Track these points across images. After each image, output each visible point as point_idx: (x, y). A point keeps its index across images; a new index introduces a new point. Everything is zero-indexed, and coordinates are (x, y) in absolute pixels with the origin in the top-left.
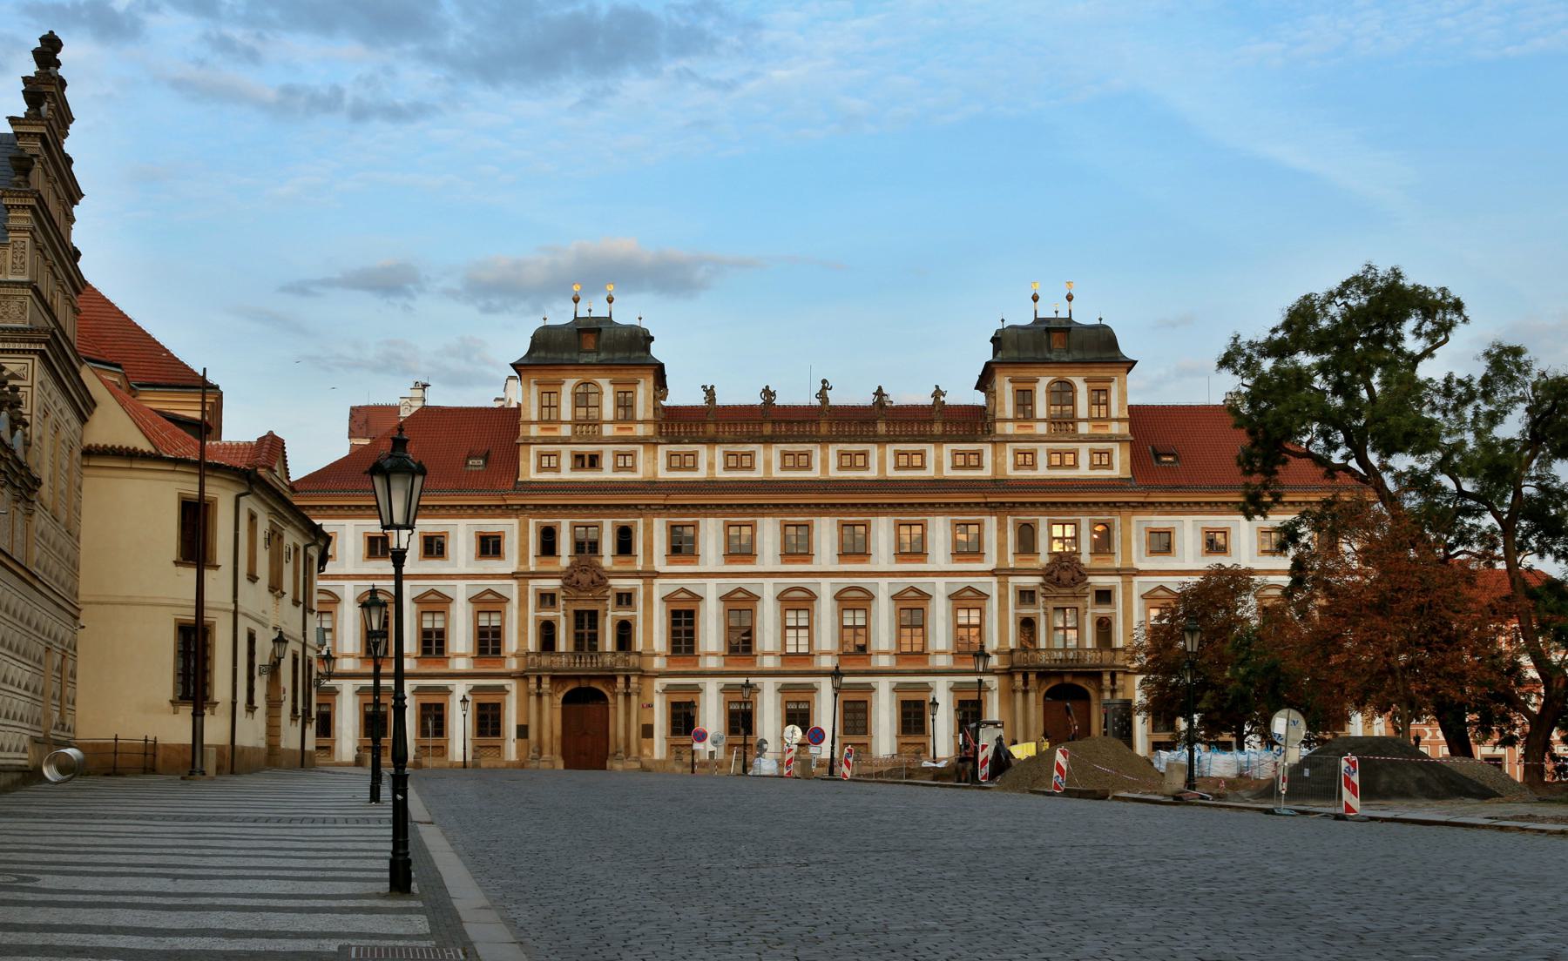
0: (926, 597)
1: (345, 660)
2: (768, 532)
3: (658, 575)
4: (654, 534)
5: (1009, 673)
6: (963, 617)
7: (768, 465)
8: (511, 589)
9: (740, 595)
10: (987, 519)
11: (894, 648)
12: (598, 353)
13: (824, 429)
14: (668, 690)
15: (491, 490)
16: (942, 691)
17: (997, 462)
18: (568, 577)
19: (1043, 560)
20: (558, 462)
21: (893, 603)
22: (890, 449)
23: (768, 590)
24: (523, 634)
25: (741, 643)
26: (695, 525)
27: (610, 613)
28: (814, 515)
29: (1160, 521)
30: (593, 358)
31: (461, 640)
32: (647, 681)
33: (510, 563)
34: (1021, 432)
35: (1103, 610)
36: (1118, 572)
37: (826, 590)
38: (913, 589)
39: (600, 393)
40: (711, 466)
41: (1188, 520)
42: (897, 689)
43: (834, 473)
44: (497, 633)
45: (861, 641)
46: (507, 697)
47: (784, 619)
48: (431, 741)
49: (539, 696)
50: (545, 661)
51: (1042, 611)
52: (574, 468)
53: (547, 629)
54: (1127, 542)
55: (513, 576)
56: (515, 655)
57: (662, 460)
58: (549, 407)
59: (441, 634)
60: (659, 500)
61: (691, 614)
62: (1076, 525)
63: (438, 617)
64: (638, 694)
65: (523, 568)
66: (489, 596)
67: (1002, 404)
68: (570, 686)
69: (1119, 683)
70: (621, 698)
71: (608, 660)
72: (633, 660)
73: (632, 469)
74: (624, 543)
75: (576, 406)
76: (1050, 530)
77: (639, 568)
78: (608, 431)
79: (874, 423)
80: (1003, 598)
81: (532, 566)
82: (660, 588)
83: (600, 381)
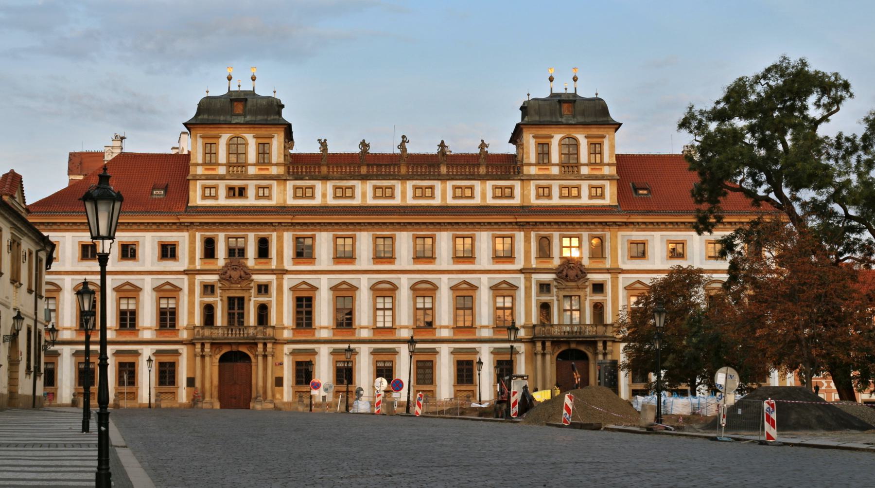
0: (474, 288)
1: (65, 332)
2: (364, 241)
3: (287, 272)
4: (284, 244)
5: (532, 341)
6: (500, 301)
7: (364, 195)
8: (183, 282)
9: (344, 286)
11: (452, 324)
12: (245, 116)
13: (403, 170)
14: (294, 353)
15: (169, 212)
16: (486, 355)
17: (524, 194)
18: (223, 273)
19: (556, 262)
20: (217, 192)
21: (451, 292)
22: (450, 184)
23: (364, 283)
24: (191, 313)
25: (345, 320)
26: (313, 238)
27: (253, 299)
28: (396, 230)
29: (638, 235)
30: (241, 120)
31: (147, 318)
32: (279, 347)
34: (541, 173)
35: (598, 298)
36: (608, 271)
37: (404, 283)
39: (246, 144)
40: (324, 195)
42: (454, 352)
43: (410, 201)
44: (173, 313)
45: (429, 319)
46: (180, 358)
47: (375, 303)
48: (126, 389)
49: (203, 357)
50: (207, 332)
51: (555, 298)
52: (228, 197)
53: (209, 311)
54: (614, 250)
55: (185, 272)
56: (186, 328)
58: (210, 152)
59: (133, 313)
60: (287, 219)
61: (310, 300)
62: (579, 237)
63: (131, 301)
64: (273, 356)
65: (192, 267)
66: (168, 287)
67: (528, 153)
68: (225, 350)
69: (609, 348)
70: (260, 359)
71: (251, 332)
72: (269, 331)
73: (269, 197)
74: (263, 250)
75: (229, 154)
76: (561, 242)
77: (274, 267)
78: (252, 171)
79: (439, 167)
80: (528, 289)
81: (198, 265)
82: (288, 281)
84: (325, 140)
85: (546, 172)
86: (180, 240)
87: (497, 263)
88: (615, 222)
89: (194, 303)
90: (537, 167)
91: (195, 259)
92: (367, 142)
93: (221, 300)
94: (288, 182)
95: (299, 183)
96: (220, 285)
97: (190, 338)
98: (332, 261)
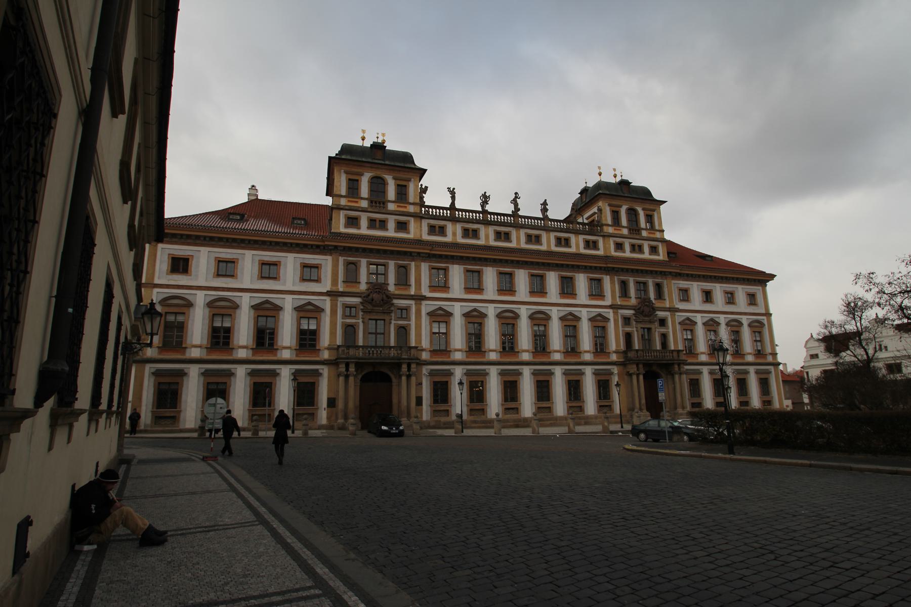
1: (193, 349)
8: (326, 303)
9: (475, 313)
10: (604, 276)
18: (367, 298)
27: (393, 322)
29: (683, 284)
31: (287, 335)
33: (326, 285)
34: (616, 232)
35: (663, 330)
38: (571, 314)
39: (384, 183)
40: (454, 234)
41: (695, 284)
48: (259, 410)
49: (347, 377)
50: (352, 352)
53: (349, 330)
55: (328, 294)
56: (328, 349)
57: (425, 229)
64: (415, 375)
65: (334, 289)
66: (310, 307)
67: (606, 216)
70: (404, 378)
71: (393, 353)
72: (413, 351)
75: (372, 191)
77: (413, 293)
78: (391, 207)
80: (616, 321)
83: (386, 176)
86: (323, 263)
87: (592, 299)
88: (670, 273)
89: (336, 324)
93: (363, 322)
94: (423, 220)
95: (433, 222)
97: (333, 358)
98: (463, 290)
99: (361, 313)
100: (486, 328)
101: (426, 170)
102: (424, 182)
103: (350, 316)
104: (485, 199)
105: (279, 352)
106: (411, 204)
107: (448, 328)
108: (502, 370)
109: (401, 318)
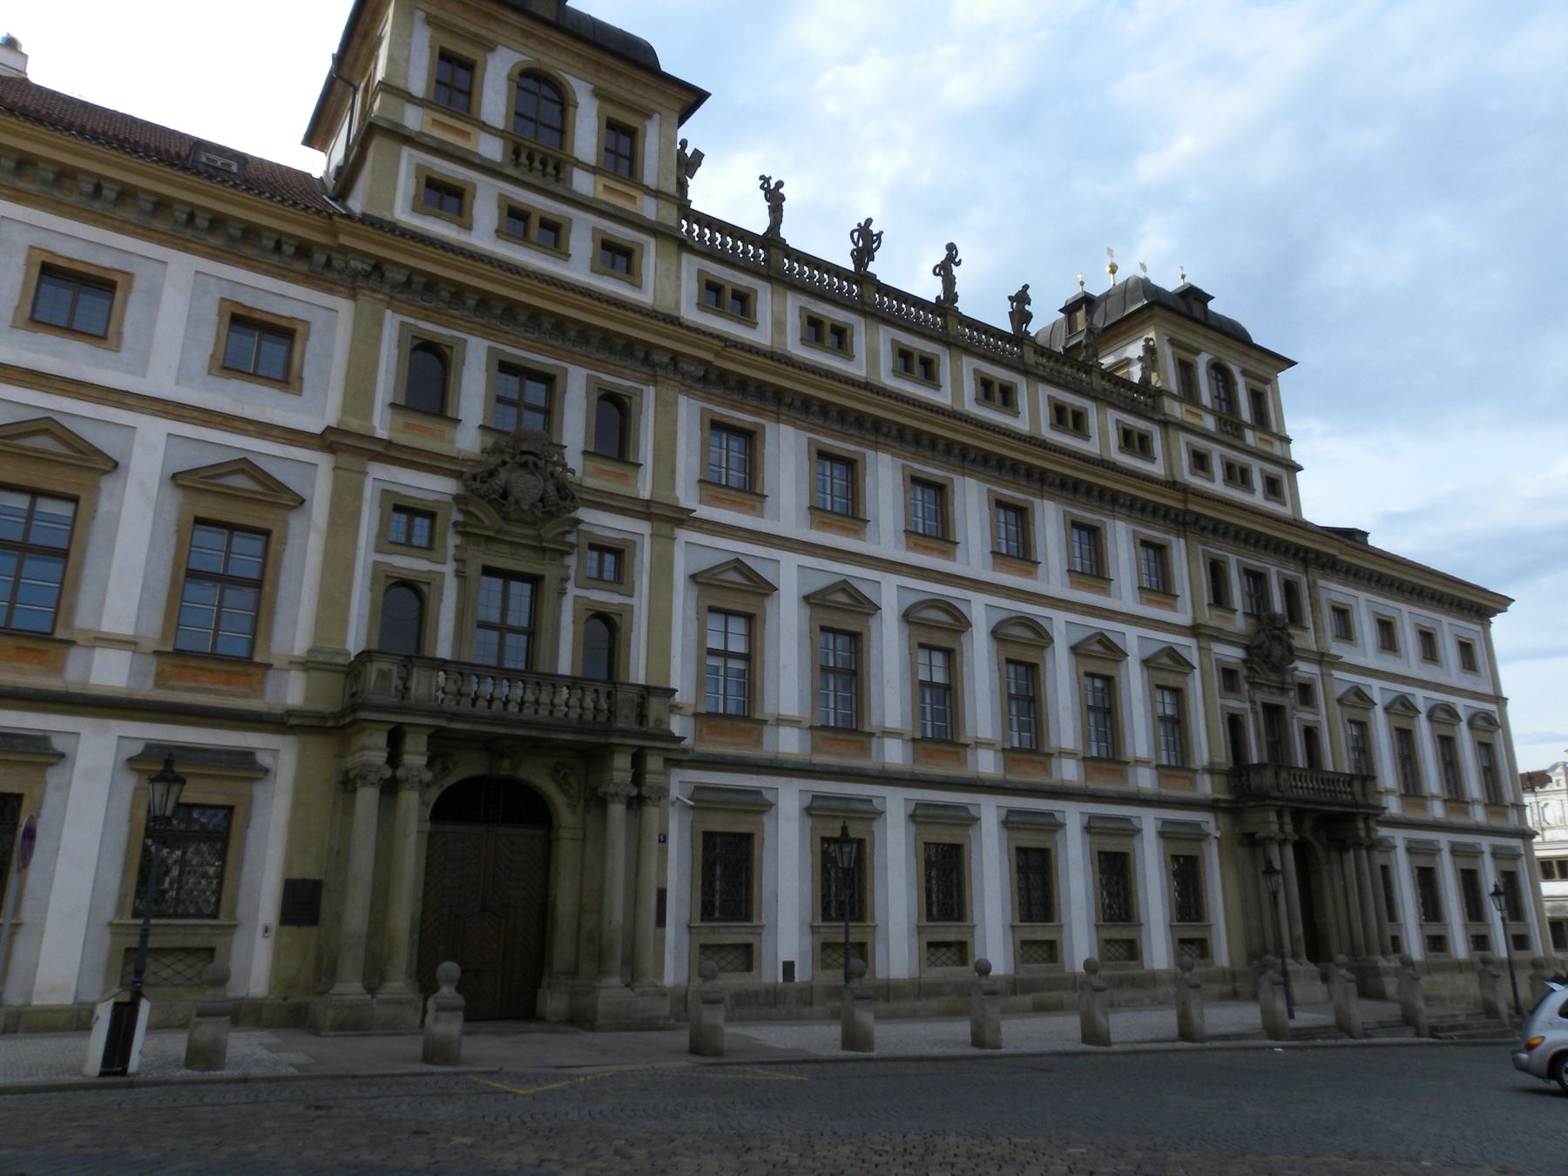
4: (675, 431)
14: (703, 800)
27: (572, 590)
33: (318, 408)
35: (1307, 716)
39: (564, 102)
40: (779, 325)
46: (259, 790)
49: (390, 789)
51: (1248, 705)
52: (500, 233)
55: (329, 441)
65: (355, 425)
68: (468, 767)
73: (635, 282)
77: (645, 493)
81: (381, 424)
82: (691, 552)
83: (567, 76)
84: (780, 184)
85: (1196, 421)
86: (318, 321)
87: (1149, 602)
89: (350, 567)
90: (1185, 407)
91: (371, 402)
92: (874, 229)
93: (459, 574)
94: (685, 257)
96: (457, 516)
98: (805, 514)
99: (453, 540)
100: (874, 653)
101: (700, 96)
102: (693, 132)
103: (408, 545)
104: (866, 241)
105: (75, 659)
106: (647, 191)
107: (751, 637)
108: (920, 805)
109: (598, 581)
